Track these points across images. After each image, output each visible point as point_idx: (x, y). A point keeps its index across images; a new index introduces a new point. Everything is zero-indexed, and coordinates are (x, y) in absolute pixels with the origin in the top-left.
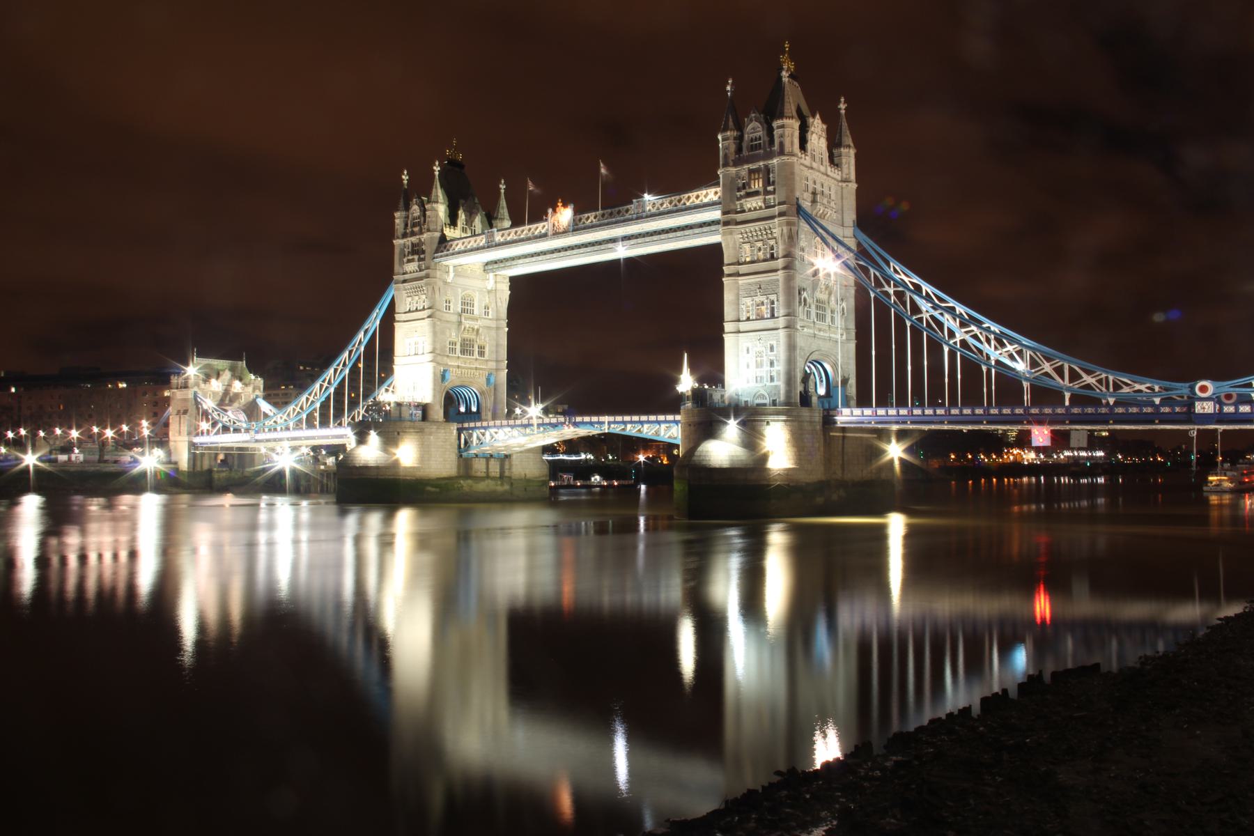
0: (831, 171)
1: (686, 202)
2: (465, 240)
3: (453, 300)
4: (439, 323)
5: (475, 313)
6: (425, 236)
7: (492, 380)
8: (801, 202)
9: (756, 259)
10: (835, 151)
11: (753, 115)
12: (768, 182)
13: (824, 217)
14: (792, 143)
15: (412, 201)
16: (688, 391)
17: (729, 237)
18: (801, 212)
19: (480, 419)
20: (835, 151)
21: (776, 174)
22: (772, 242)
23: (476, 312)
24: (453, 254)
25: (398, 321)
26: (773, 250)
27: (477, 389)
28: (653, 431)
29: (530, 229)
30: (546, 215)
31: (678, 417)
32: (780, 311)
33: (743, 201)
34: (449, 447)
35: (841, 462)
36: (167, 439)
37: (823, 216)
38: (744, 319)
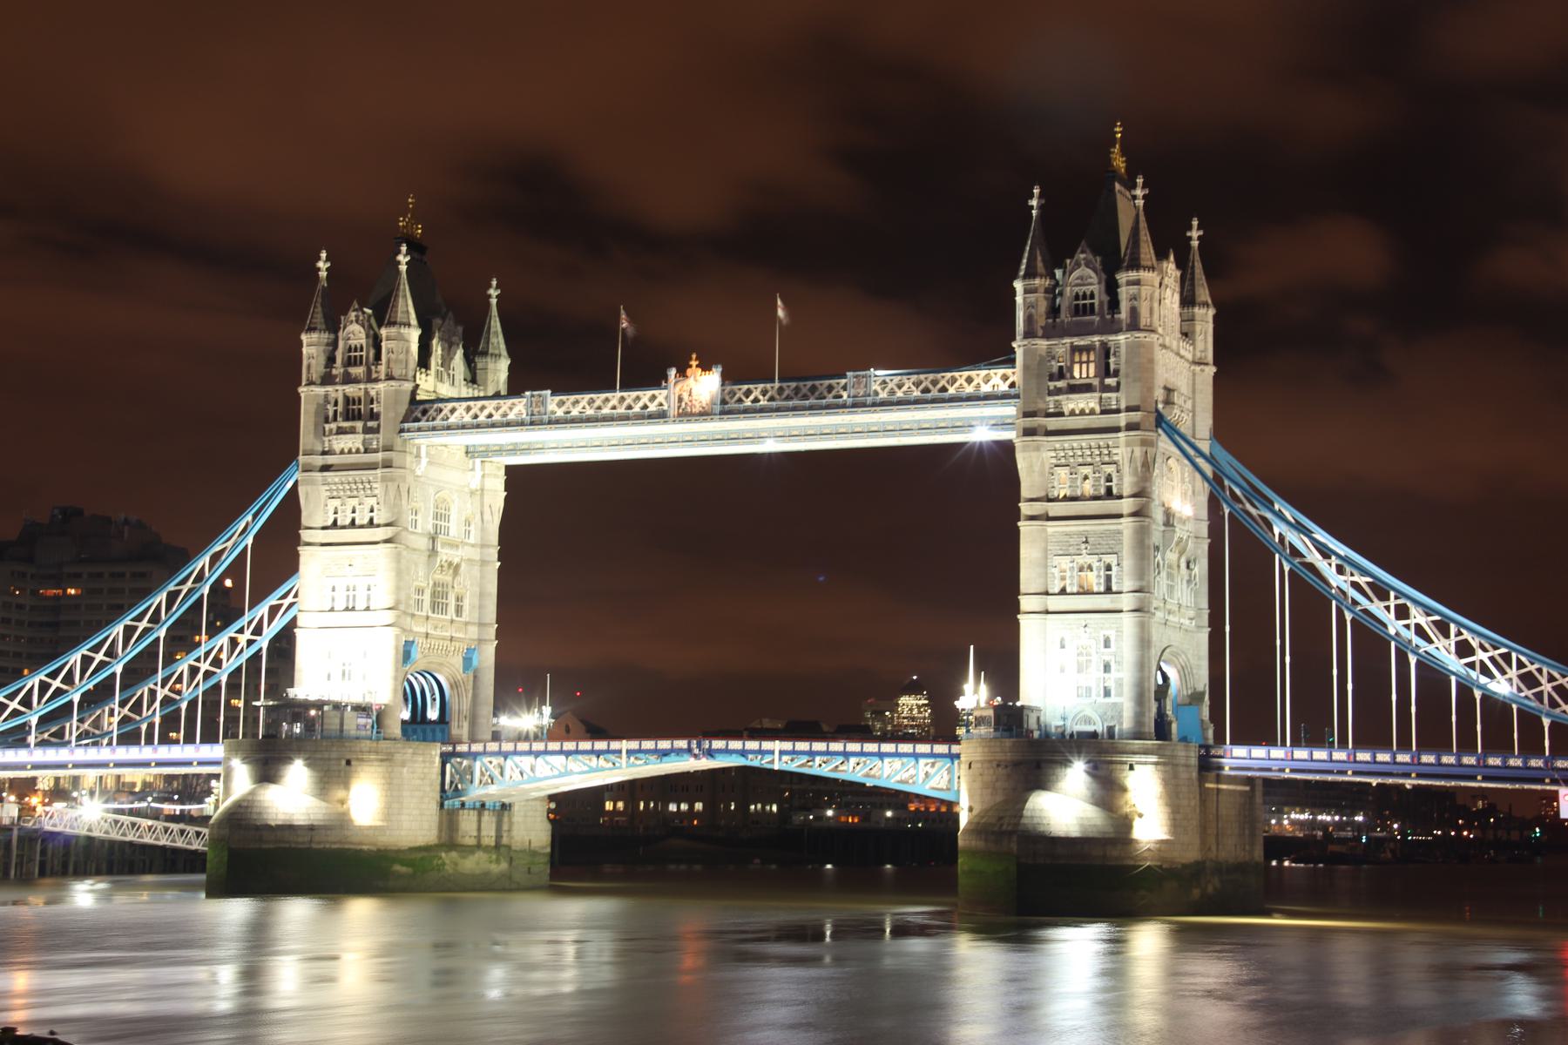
2: (471, 403)
3: (423, 509)
4: (405, 553)
7: (475, 663)
9: (1079, 493)
11: (1082, 256)
12: (1105, 371)
17: (1034, 454)
18: (1164, 425)
22: (1110, 469)
24: (449, 428)
26: (1111, 481)
27: (448, 679)
30: (666, 379)
32: (1128, 584)
34: (428, 789)
35: (1215, 832)
38: (1057, 590)
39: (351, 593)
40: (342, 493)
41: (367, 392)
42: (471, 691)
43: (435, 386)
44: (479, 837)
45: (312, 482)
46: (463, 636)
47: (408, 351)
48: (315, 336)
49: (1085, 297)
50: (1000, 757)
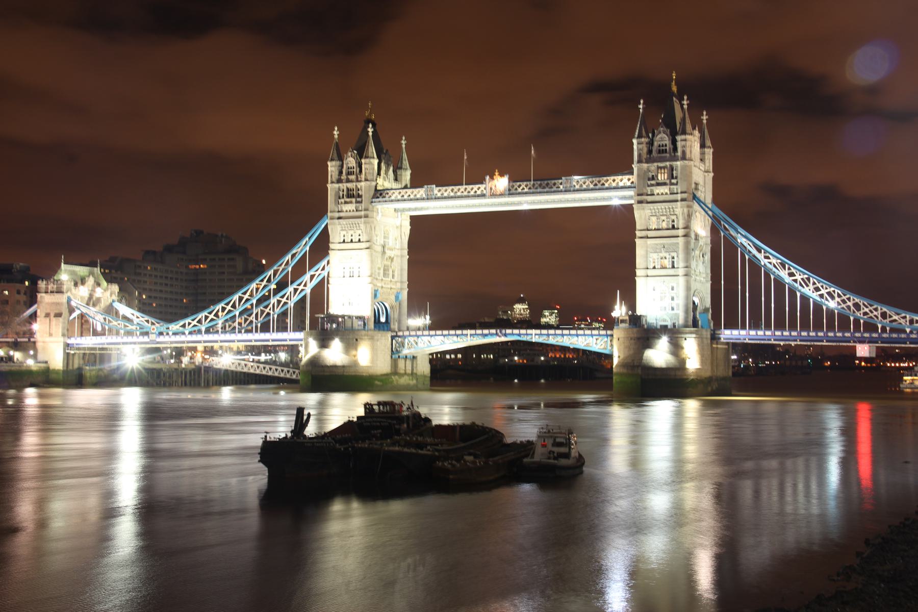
5: (390, 244)
7: (400, 298)
9: (661, 227)
11: (662, 129)
12: (672, 177)
15: (347, 153)
17: (642, 211)
18: (696, 199)
22: (674, 217)
23: (391, 244)
24: (392, 201)
32: (681, 264)
38: (652, 267)
43: (383, 183)
44: (405, 370)
45: (334, 224)
47: (373, 169)
48: (334, 163)
49: (663, 146)
50: (632, 336)
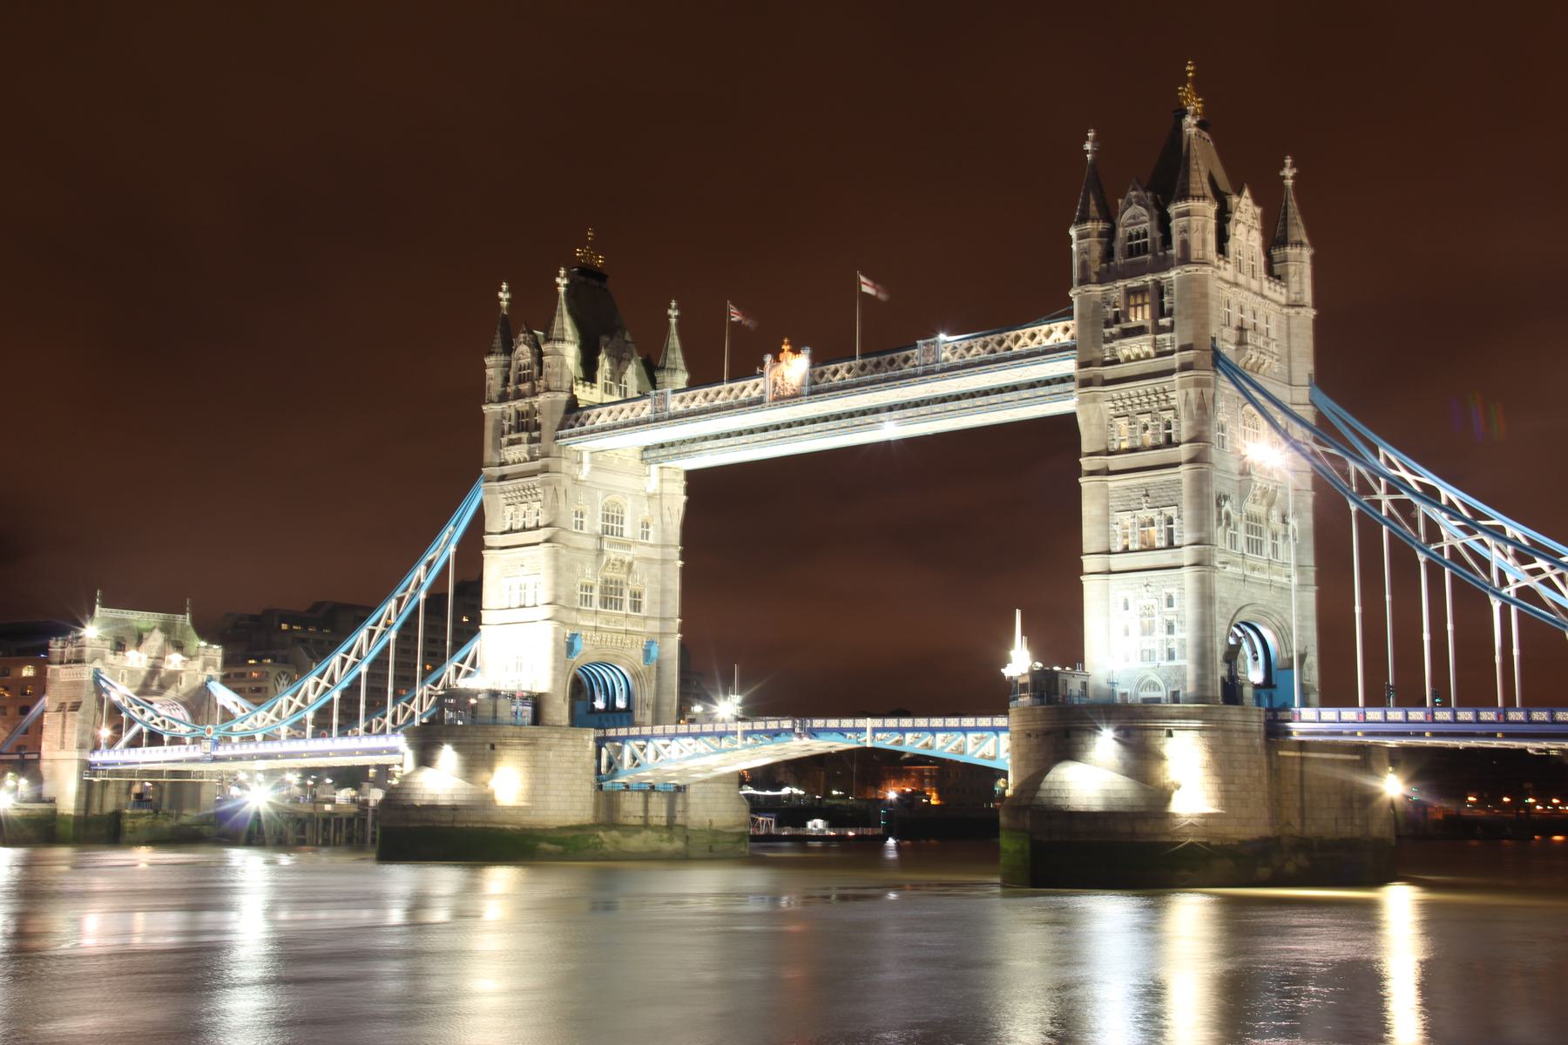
0: (1270, 288)
1: (1013, 346)
2: (612, 407)
3: (589, 513)
4: (564, 551)
5: (625, 534)
6: (542, 399)
7: (654, 653)
8: (1219, 344)
9: (1138, 443)
10: (1276, 253)
11: (1133, 193)
12: (1160, 312)
13: (1258, 368)
14: (1204, 242)
15: (517, 336)
16: (1023, 675)
17: (1090, 406)
18: (1221, 363)
19: (631, 723)
20: (1276, 253)
21: (1175, 292)
22: (1168, 415)
23: (628, 533)
24: (592, 432)
25: (490, 548)
26: (1170, 428)
27: (628, 670)
28: (952, 746)
29: (731, 390)
30: (762, 365)
31: (1000, 721)
32: (1184, 535)
33: (1115, 344)
34: (580, 771)
35: (1298, 805)
36: (35, 756)
37: (1257, 367)
38: (1119, 548)
39: (523, 591)
40: (515, 500)
41: (531, 405)
42: (654, 682)
43: (602, 398)
44: (646, 817)
46: (642, 630)
50: (1033, 726)
